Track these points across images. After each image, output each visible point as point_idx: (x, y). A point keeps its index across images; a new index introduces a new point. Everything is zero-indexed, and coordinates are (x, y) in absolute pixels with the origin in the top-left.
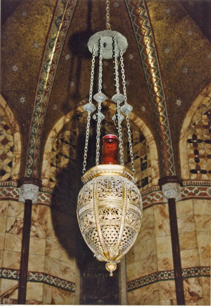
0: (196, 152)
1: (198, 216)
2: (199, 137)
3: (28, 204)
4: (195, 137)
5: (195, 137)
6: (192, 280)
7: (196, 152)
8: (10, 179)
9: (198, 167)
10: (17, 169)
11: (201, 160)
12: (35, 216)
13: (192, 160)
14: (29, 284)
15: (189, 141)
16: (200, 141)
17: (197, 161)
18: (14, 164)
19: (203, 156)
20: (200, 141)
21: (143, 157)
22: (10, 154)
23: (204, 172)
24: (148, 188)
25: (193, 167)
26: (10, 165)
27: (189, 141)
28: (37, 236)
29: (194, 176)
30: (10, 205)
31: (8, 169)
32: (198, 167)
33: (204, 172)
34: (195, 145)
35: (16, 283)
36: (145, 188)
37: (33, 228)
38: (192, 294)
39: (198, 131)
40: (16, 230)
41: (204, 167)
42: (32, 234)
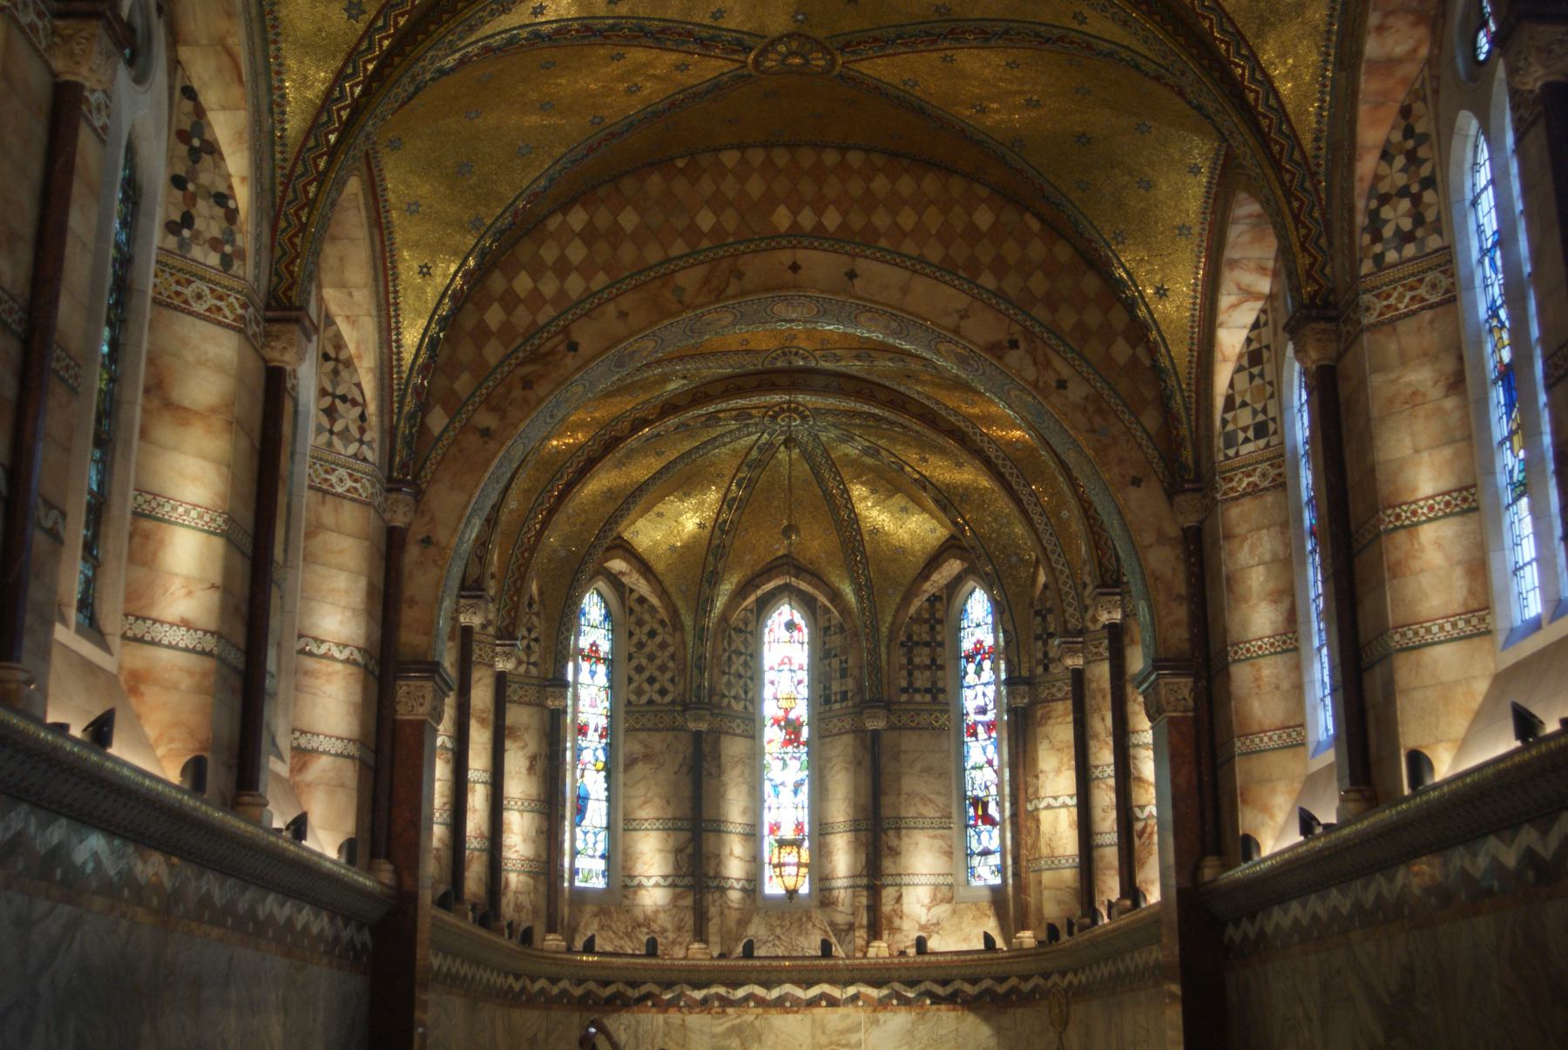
0: (910, 661)
1: (906, 752)
2: (915, 638)
3: (698, 736)
4: (910, 637)
5: (910, 637)
6: (891, 833)
7: (910, 661)
8: (673, 702)
9: (911, 684)
10: (681, 688)
11: (916, 673)
12: (707, 749)
13: (904, 673)
14: (704, 835)
15: (903, 644)
16: (917, 644)
17: (910, 674)
18: (677, 679)
19: (917, 667)
20: (917, 644)
21: (843, 658)
22: (671, 664)
23: (917, 691)
24: (847, 707)
25: (904, 684)
26: (672, 680)
27: (903, 644)
28: (710, 774)
29: (904, 698)
30: (676, 737)
31: (670, 687)
32: (911, 684)
33: (917, 691)
34: (910, 651)
35: (688, 835)
36: (844, 705)
37: (705, 765)
38: (890, 848)
39: (915, 628)
40: (685, 769)
41: (918, 684)
42: (705, 772)
